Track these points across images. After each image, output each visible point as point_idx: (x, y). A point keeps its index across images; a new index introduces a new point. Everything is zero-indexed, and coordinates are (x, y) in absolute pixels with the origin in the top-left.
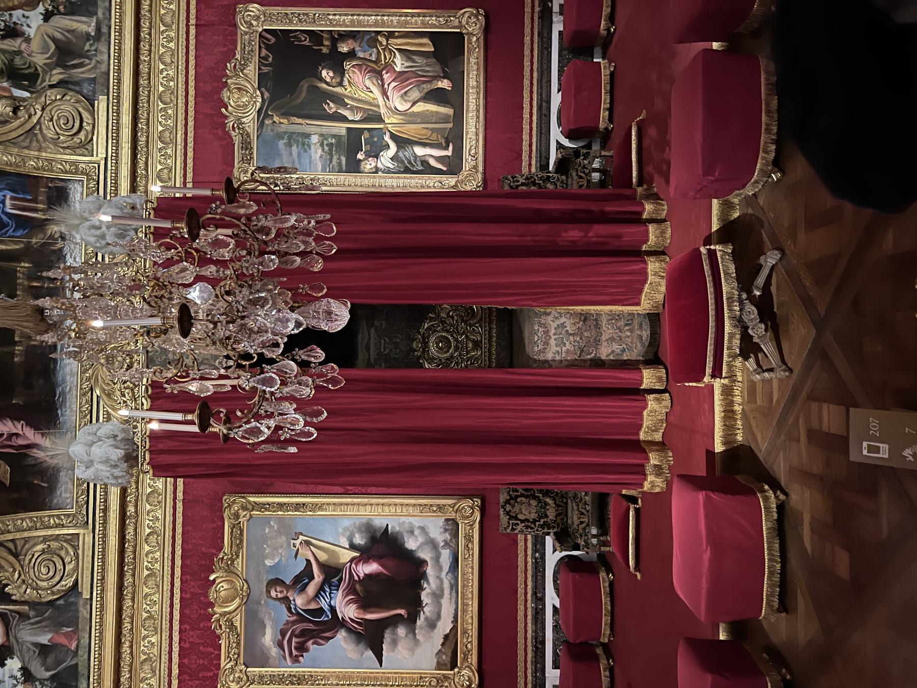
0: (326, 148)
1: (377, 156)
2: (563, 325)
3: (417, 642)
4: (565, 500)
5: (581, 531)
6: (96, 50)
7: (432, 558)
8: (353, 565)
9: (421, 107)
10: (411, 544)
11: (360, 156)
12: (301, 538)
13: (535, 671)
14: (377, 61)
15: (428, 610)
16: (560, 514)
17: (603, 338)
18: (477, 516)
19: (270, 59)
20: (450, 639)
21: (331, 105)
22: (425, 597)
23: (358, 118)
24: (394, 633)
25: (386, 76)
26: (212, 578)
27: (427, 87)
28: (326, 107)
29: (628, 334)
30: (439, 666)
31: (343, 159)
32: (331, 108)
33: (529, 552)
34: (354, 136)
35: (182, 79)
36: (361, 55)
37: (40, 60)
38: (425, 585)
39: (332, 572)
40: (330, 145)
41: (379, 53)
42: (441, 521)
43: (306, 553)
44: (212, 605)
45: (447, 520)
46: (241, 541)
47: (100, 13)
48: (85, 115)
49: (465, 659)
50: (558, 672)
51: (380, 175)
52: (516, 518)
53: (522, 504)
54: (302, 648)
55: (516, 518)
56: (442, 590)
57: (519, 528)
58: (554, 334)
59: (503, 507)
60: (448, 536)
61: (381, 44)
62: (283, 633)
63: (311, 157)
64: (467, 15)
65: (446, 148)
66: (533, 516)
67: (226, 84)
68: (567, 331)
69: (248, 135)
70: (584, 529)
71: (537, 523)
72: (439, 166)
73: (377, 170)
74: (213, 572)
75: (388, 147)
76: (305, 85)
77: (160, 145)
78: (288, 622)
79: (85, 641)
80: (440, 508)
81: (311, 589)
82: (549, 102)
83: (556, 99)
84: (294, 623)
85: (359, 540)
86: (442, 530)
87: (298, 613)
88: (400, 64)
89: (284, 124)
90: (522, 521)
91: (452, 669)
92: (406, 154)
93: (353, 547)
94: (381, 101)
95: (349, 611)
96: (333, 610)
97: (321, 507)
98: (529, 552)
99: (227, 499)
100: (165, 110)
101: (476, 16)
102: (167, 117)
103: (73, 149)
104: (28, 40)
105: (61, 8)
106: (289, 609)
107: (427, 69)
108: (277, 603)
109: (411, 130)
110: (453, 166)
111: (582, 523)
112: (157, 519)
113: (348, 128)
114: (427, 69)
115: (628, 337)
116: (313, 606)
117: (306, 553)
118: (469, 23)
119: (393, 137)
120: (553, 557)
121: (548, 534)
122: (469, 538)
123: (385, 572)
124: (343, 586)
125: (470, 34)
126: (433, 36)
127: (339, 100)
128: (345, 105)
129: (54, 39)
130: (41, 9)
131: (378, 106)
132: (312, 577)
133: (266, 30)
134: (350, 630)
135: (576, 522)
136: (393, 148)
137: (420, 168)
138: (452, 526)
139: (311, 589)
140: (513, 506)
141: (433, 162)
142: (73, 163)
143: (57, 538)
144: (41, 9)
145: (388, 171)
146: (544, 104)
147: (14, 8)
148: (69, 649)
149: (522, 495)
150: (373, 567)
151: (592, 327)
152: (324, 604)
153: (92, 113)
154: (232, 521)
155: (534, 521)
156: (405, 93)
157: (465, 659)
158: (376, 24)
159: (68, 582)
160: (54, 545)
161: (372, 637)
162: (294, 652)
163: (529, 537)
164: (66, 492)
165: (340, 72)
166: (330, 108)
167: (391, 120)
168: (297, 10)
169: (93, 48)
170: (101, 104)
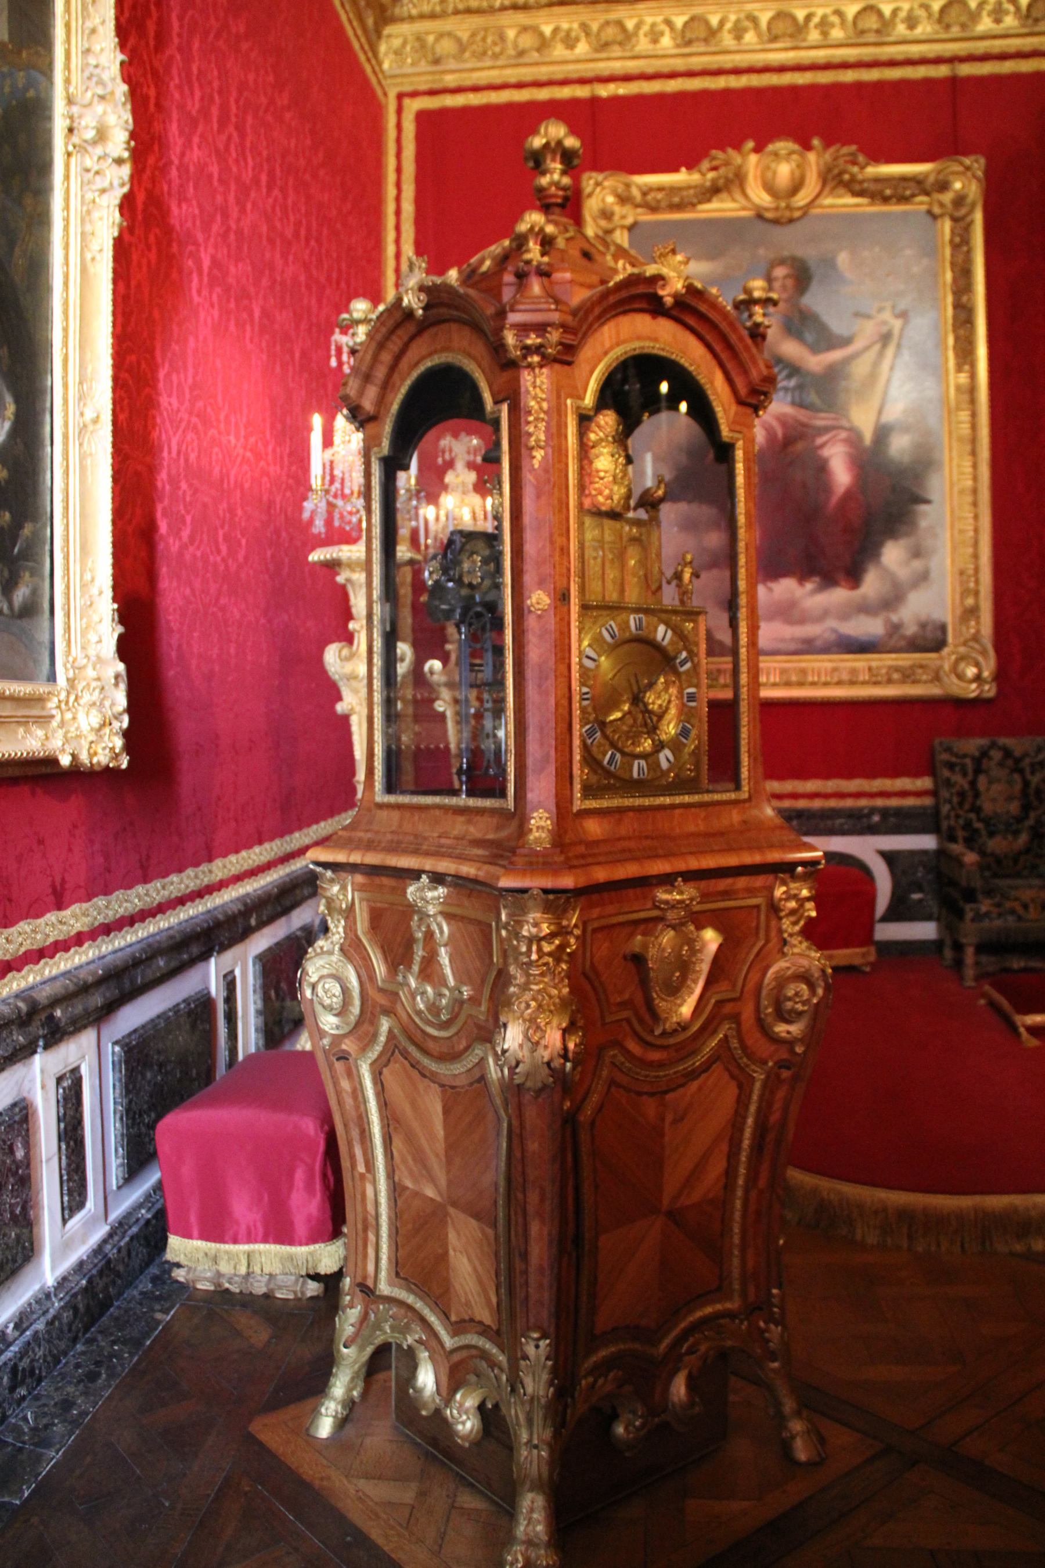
4: (1025, 873)
5: (1008, 905)
7: (864, 598)
8: (843, 435)
12: (897, 324)
16: (999, 862)
33: (879, 802)
38: (809, 586)
42: (947, 615)
45: (943, 628)
46: (886, 200)
52: (978, 771)
53: (1010, 782)
55: (978, 771)
56: (802, 621)
57: (957, 778)
59: (993, 745)
60: (911, 630)
66: (988, 807)
70: (1013, 912)
80: (972, 612)
86: (923, 618)
90: (973, 784)
98: (879, 802)
111: (1025, 907)
135: (1027, 895)
138: (931, 639)
140: (1001, 764)
149: (1026, 784)
154: (932, 179)
155: (976, 810)
163: (928, 801)
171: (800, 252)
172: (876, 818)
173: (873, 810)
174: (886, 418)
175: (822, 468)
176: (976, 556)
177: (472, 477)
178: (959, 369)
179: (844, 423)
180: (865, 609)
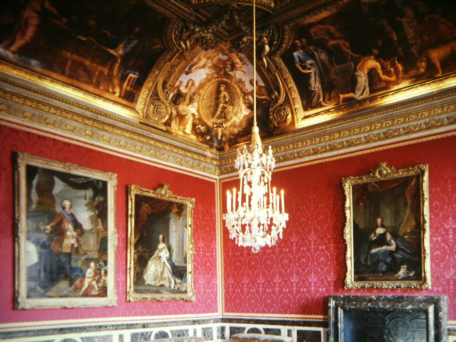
37: (181, 107)
104: (188, 105)
105: (195, 121)
129: (186, 115)
130: (196, 114)
144: (196, 114)
147: (198, 104)
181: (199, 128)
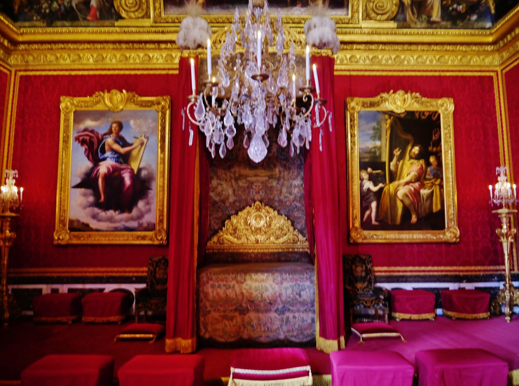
0: (373, 150)
1: (370, 179)
2: (267, 290)
3: (85, 208)
6: (422, 21)
7: (133, 216)
9: (400, 205)
10: (141, 204)
11: (369, 170)
12: (145, 140)
13: (67, 278)
14: (426, 179)
15: (103, 214)
17: (260, 315)
18: (156, 242)
19: (423, 117)
20: (86, 227)
21: (399, 153)
22: (111, 213)
23: (392, 168)
24: (90, 195)
25: (417, 185)
26: (124, 91)
27: (412, 209)
28: (397, 149)
29: (263, 329)
30: (71, 222)
31: (367, 160)
32: (397, 152)
34: (381, 166)
35: (409, 68)
36: (429, 169)
38: (117, 212)
39: (124, 158)
40: (375, 152)
41: (430, 180)
42: (153, 221)
43: (136, 143)
44: (109, 92)
46: (144, 107)
47: (444, 23)
48: (385, 17)
49: (75, 236)
50: (66, 291)
51: (360, 181)
54: (83, 142)
55: (157, 266)
56: (115, 222)
57: (151, 268)
58: (262, 286)
60: (145, 225)
61: (435, 181)
62: (92, 131)
63: (368, 141)
64: (455, 231)
65: (376, 220)
66: (158, 276)
67: (406, 92)
68: (264, 293)
69: (378, 105)
71: (153, 279)
72: (366, 216)
73: (362, 179)
74: (127, 91)
75: (375, 185)
76: (409, 137)
77: (371, 57)
78: (98, 134)
79: (91, 24)
80: (161, 221)
81: (116, 147)
82: (406, 281)
83: (408, 286)
84: (98, 137)
85: (144, 173)
86: (149, 221)
87: (103, 139)
88: (424, 192)
89: (386, 125)
91: (69, 229)
92: (372, 198)
93: (140, 170)
94: (403, 181)
95: (103, 168)
96: (104, 159)
97: (163, 150)
98: (135, 274)
99: (168, 98)
100: (391, 59)
101: (455, 237)
102: (387, 60)
103: (366, 10)
106: (105, 134)
107: (423, 209)
108: (109, 127)
109: (386, 200)
110: (366, 225)
111: (152, 305)
112: (157, 60)
113: (385, 163)
114: (423, 209)
115: (261, 329)
116: (107, 148)
117: (136, 143)
118: (451, 233)
119: (381, 189)
120: (132, 288)
121: (147, 285)
122: (144, 238)
123: (126, 188)
124: (118, 165)
125: (444, 234)
126: (442, 212)
127: (401, 157)
128: (399, 160)
131: (399, 179)
132: (123, 147)
133: (439, 115)
134: (92, 169)
136: (375, 189)
137: (364, 205)
138: (151, 227)
139: (116, 147)
141: (368, 213)
142: (358, 11)
143: (148, 7)
145: (361, 186)
146: (405, 279)
148: (87, 16)
150: (128, 181)
151: (266, 308)
152: (108, 154)
153: (387, 20)
155: (155, 277)
156: (407, 196)
157: (75, 236)
158: (447, 178)
159: (124, 14)
160: (144, 7)
161: (88, 182)
162: (81, 138)
163: (145, 274)
164: (173, 13)
165: (418, 157)
166: (397, 152)
167: (391, 187)
168: (452, 132)
169: (423, 20)
170: (392, 24)
171: (120, 120)
172: (134, 279)
173: (133, 277)
174: (141, 166)
175: (122, 179)
176: (163, 205)
177: (14, 181)
178: (161, 153)
179: (129, 167)
180: (132, 219)
181: (455, 10)
